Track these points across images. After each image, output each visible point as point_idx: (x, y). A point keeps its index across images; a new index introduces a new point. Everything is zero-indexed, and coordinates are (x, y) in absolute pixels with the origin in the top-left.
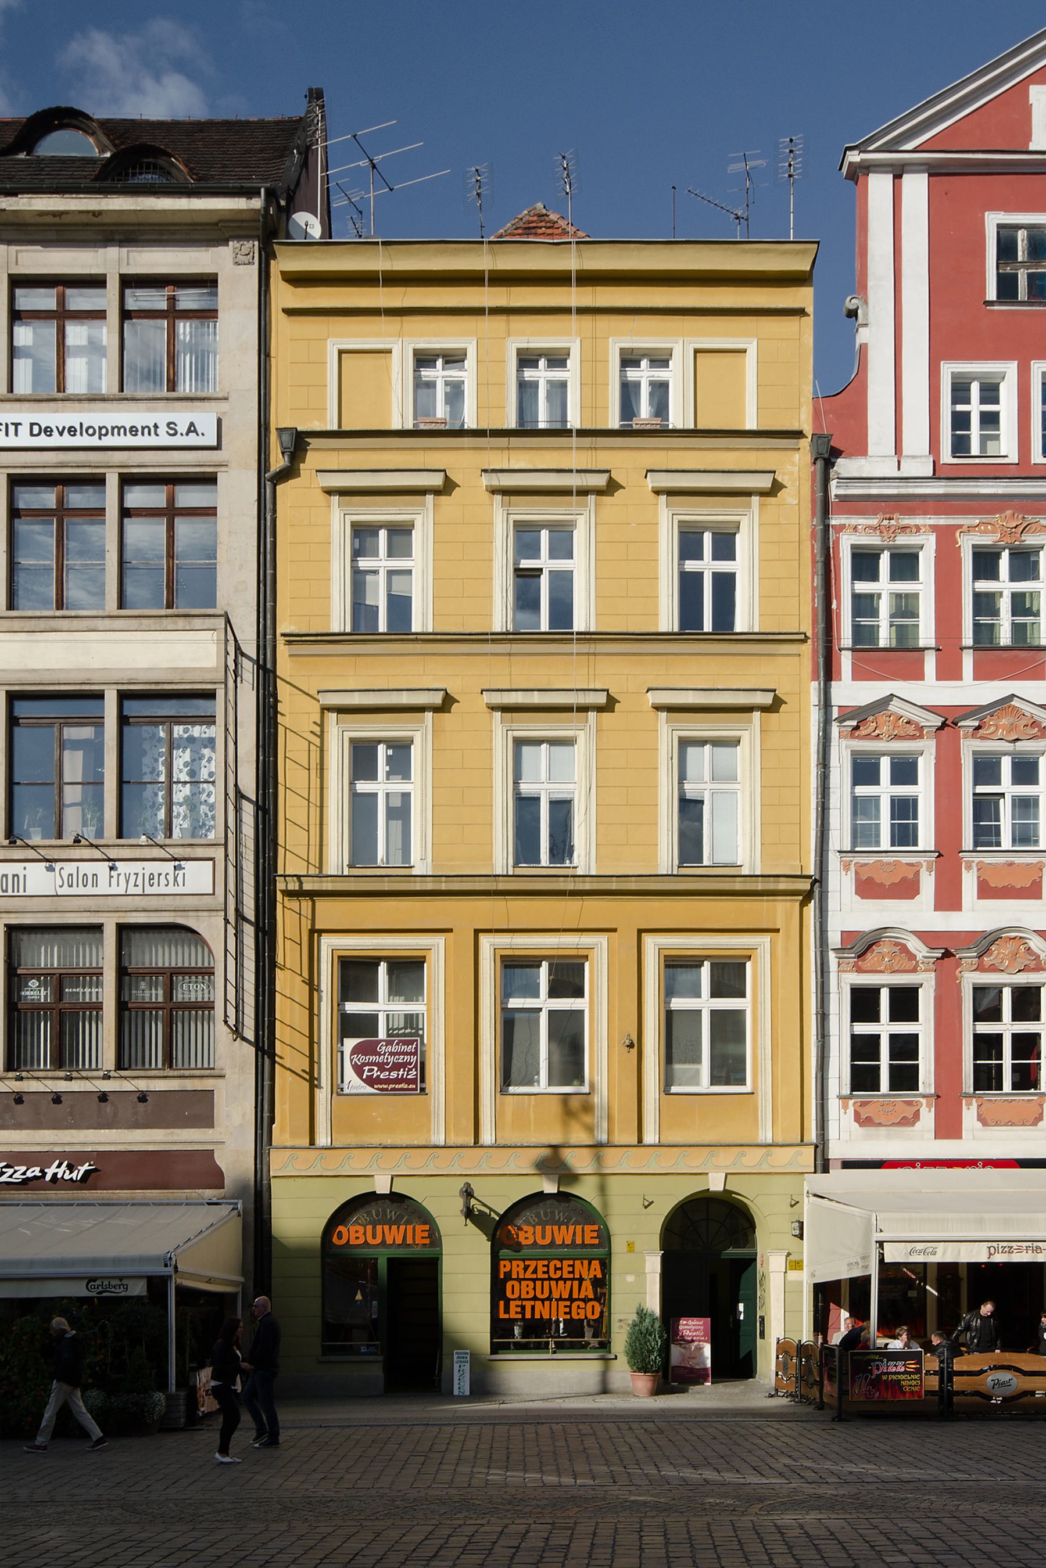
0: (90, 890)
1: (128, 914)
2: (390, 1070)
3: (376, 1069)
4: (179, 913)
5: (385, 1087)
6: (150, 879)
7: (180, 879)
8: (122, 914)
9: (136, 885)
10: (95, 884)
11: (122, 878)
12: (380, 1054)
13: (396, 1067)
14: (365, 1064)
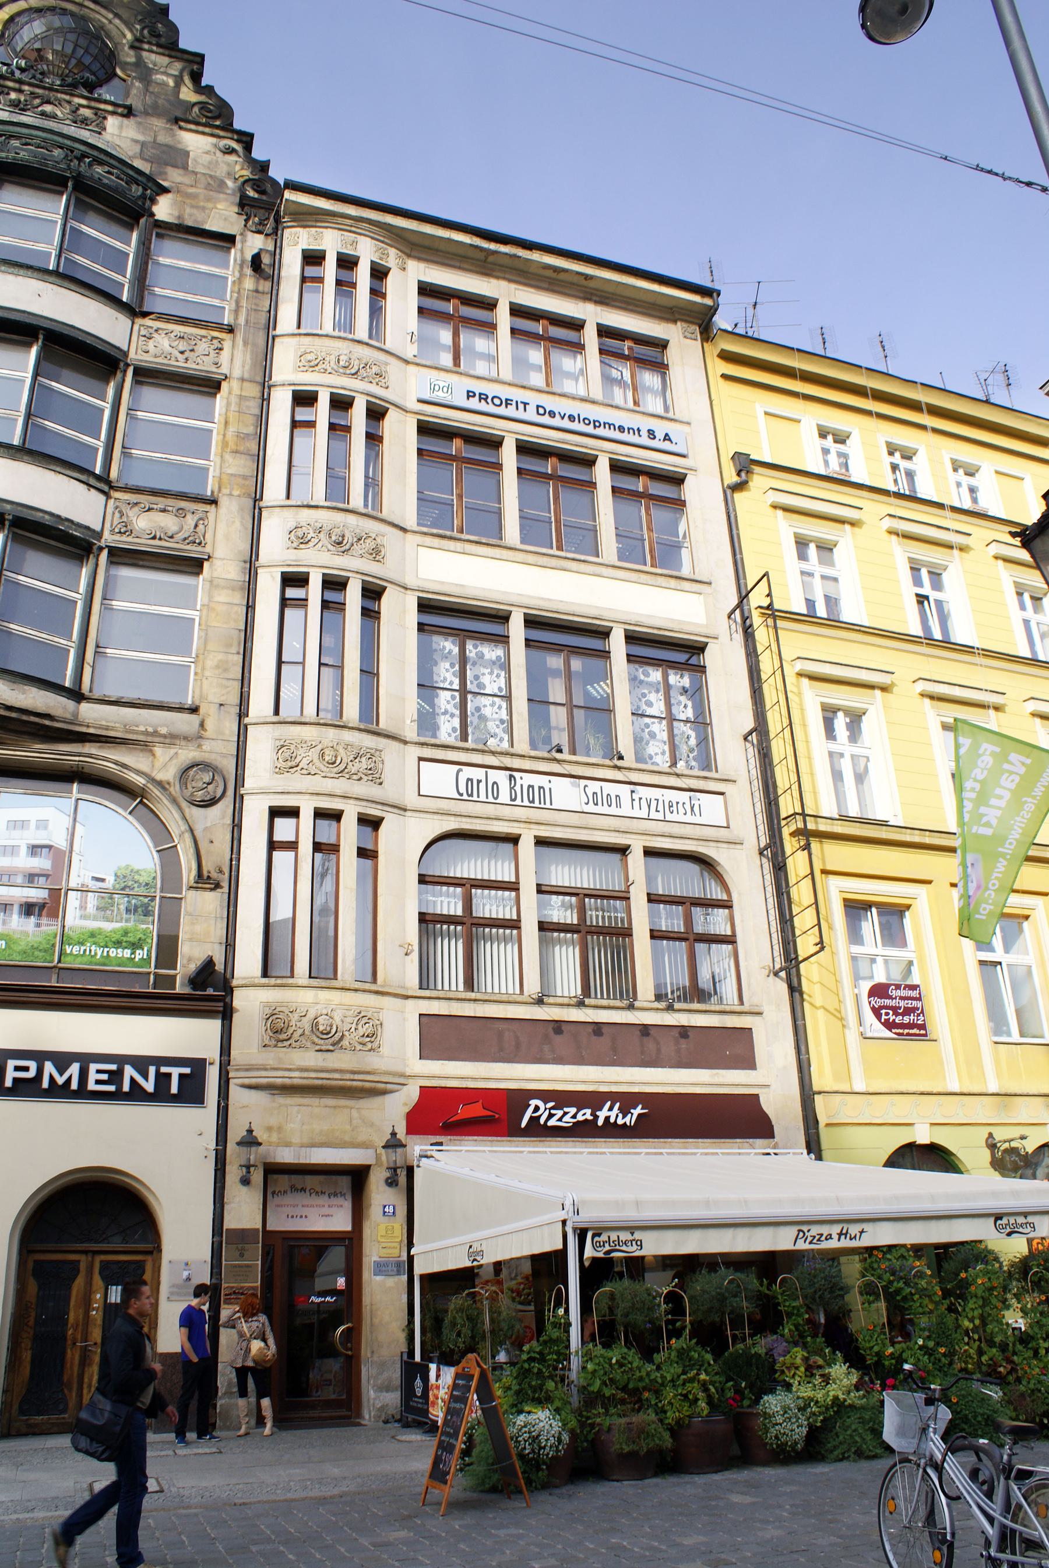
0: (613, 810)
1: (654, 838)
2: (903, 1014)
3: (891, 1012)
4: (701, 843)
5: (901, 1031)
6: (670, 807)
7: (696, 809)
8: (648, 838)
9: (657, 811)
10: (619, 805)
11: (644, 803)
12: (891, 998)
13: (908, 1011)
14: (881, 1008)
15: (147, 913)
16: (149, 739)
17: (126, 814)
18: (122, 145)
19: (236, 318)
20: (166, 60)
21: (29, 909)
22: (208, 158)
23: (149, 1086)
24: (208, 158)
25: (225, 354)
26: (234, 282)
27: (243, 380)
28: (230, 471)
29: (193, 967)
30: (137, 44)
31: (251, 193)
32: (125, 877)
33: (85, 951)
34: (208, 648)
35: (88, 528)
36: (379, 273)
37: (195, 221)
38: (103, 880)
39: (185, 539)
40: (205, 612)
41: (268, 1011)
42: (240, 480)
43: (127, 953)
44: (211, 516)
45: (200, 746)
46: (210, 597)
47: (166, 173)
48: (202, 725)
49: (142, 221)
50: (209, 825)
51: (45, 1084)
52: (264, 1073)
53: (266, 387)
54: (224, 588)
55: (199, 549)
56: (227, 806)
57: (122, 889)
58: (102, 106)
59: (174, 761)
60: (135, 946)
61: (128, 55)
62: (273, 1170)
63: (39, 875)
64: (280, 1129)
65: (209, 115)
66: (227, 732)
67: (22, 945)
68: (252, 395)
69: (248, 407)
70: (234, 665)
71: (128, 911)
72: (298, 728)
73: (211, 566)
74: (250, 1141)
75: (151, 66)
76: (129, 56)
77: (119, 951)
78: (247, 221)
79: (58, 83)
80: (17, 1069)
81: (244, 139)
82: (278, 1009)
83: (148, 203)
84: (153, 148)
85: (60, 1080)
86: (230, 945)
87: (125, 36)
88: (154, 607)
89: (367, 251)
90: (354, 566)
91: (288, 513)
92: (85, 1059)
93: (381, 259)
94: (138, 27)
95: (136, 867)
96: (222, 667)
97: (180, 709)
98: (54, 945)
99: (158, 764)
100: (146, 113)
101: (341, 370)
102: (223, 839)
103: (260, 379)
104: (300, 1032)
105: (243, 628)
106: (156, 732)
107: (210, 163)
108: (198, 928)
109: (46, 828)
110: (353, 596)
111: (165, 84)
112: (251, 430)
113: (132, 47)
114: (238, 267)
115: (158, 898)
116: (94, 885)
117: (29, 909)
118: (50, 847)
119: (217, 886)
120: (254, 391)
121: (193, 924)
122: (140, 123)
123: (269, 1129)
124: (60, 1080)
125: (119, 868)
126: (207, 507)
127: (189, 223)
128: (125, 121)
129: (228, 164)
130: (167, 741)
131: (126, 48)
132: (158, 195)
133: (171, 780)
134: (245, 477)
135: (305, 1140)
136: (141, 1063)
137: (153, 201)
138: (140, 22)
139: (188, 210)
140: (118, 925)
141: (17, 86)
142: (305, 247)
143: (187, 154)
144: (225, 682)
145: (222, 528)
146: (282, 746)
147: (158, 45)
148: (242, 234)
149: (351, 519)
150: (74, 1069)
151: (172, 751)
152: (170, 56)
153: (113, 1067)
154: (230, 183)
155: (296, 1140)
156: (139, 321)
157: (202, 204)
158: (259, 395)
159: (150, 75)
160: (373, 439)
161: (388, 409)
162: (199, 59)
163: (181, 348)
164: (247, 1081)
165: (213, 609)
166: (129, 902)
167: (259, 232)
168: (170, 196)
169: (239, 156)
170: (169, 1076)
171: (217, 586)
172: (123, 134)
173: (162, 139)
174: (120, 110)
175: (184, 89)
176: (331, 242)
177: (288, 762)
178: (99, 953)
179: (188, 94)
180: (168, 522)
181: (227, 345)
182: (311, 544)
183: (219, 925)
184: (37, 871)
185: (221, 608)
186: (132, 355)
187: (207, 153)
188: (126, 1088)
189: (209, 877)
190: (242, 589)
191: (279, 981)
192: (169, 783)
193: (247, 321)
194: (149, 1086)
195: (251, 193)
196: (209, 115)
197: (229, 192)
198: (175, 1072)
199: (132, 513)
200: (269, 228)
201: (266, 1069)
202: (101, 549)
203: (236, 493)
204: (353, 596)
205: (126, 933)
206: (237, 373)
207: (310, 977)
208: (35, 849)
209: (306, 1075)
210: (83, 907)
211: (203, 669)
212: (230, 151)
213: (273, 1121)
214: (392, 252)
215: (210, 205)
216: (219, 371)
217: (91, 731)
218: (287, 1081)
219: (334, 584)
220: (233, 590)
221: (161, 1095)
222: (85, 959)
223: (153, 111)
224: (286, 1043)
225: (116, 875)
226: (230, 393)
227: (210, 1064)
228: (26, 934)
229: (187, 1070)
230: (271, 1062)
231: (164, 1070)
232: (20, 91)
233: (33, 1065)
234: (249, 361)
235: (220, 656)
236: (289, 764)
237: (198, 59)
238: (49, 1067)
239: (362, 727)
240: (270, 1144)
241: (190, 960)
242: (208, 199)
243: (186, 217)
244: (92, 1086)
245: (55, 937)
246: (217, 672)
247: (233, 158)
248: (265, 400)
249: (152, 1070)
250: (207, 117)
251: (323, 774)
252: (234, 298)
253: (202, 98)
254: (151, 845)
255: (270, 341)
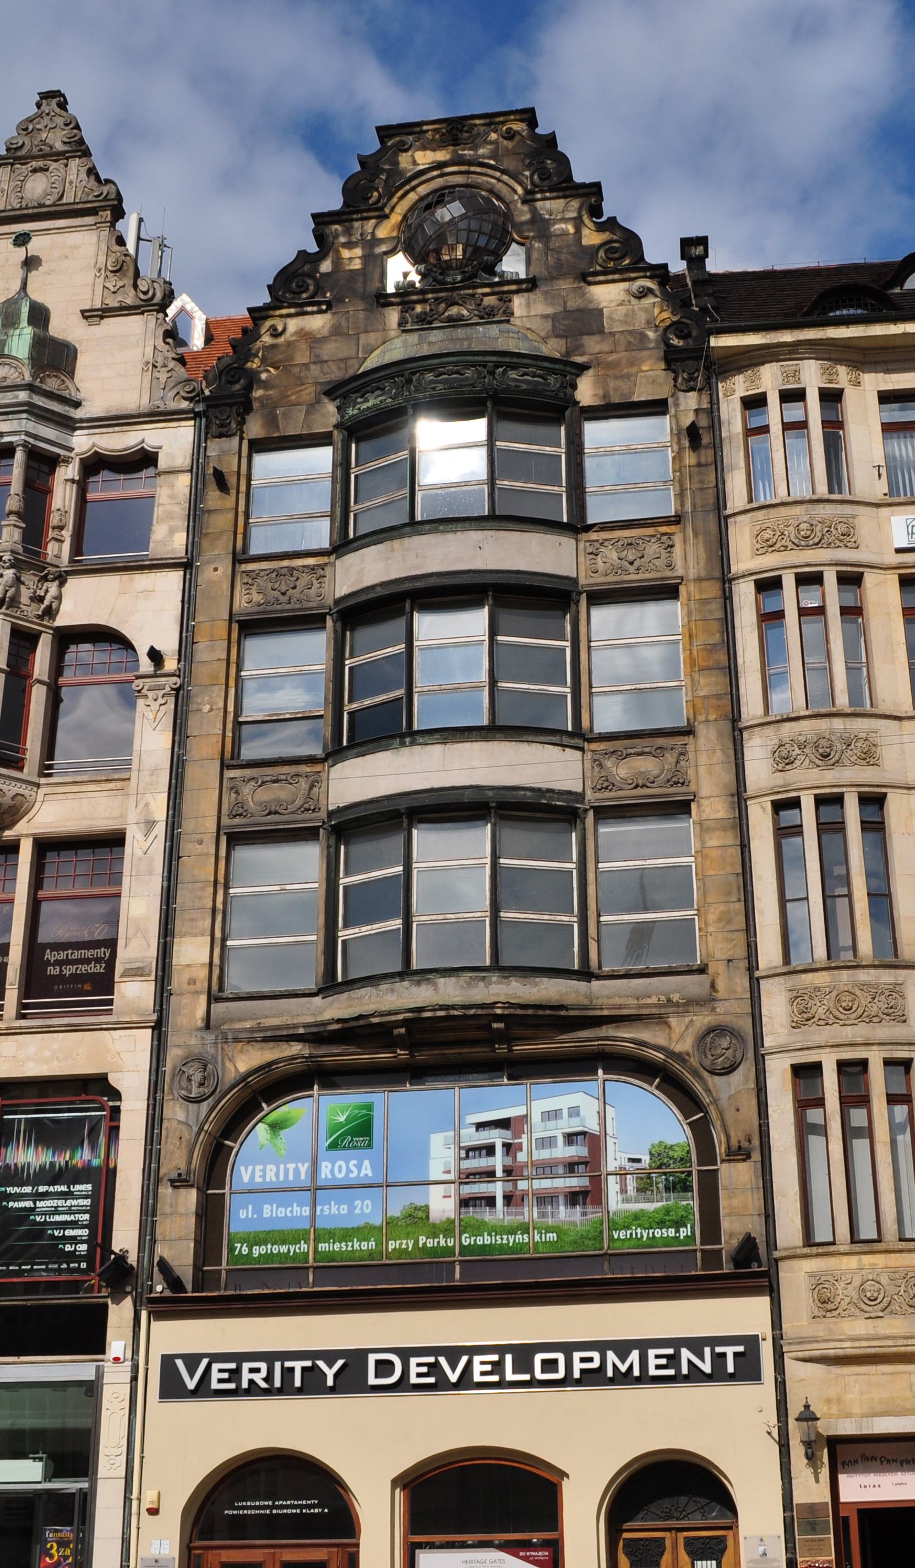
15: (687, 1188)
16: (663, 1011)
17: (652, 1089)
18: (534, 327)
19: (682, 506)
20: (561, 202)
21: (574, 1198)
22: (622, 310)
23: (707, 1368)
24: (622, 310)
25: (678, 550)
26: (674, 458)
27: (699, 580)
28: (702, 694)
29: (735, 1242)
30: (530, 197)
31: (675, 342)
32: (659, 1154)
33: (631, 1234)
34: (708, 901)
35: (569, 793)
36: (831, 397)
37: (623, 395)
38: (639, 1161)
39: (668, 781)
40: (699, 859)
41: (814, 1281)
42: (713, 702)
43: (672, 1232)
44: (690, 748)
45: (713, 1009)
46: (703, 843)
47: (582, 346)
48: (713, 986)
49: (567, 413)
50: (733, 1092)
51: (610, 1373)
52: (816, 1346)
53: (726, 581)
54: (714, 830)
55: (684, 789)
56: (749, 1070)
57: (659, 1167)
58: (506, 288)
59: (691, 1030)
60: (678, 1224)
61: (522, 213)
62: (835, 1443)
63: (578, 1164)
64: (839, 1400)
65: (616, 255)
66: (739, 989)
67: (572, 1236)
68: (712, 596)
69: (711, 612)
70: (736, 914)
71: (667, 1189)
72: (810, 975)
73: (699, 806)
74: (808, 1416)
75: (547, 217)
76: (523, 214)
77: (664, 1230)
78: (675, 380)
79: (459, 278)
80: (583, 1360)
81: (658, 272)
82: (823, 1278)
83: (569, 390)
84: (564, 319)
85: (623, 1368)
86: (769, 1215)
87: (515, 192)
88: (648, 862)
89: (811, 375)
90: (848, 776)
91: (769, 731)
92: (644, 1345)
93: (831, 382)
94: (527, 173)
95: (670, 1142)
96: (725, 918)
97: (690, 972)
98: (601, 1232)
99: (675, 1036)
100: (552, 278)
101: (803, 543)
102: (750, 1104)
103: (717, 574)
104: (847, 1300)
105: (740, 871)
106: (669, 1000)
107: (626, 315)
108: (736, 1202)
109: (578, 1115)
110: (852, 812)
111: (565, 233)
112: (717, 638)
113: (525, 202)
114: (675, 439)
115: (695, 1174)
116: (629, 1166)
117: (574, 1198)
118: (584, 1133)
119: (748, 1156)
120: (713, 590)
121: (730, 1198)
122: (547, 293)
123: (828, 1401)
124: (623, 1368)
125: (653, 1146)
126: (685, 740)
127: (615, 400)
128: (531, 296)
129: (646, 310)
130: (681, 1009)
131: (519, 205)
132: (578, 376)
133: (690, 1051)
134: (718, 696)
135: (865, 1411)
136: (696, 1345)
137: (574, 387)
138: (528, 167)
139: (612, 384)
140: (659, 1205)
141: (421, 297)
142: (742, 395)
143: (601, 311)
144: (729, 935)
145: (703, 759)
146: (797, 997)
147: (550, 191)
148: (673, 395)
149: (838, 723)
150: (635, 1356)
151: (687, 1020)
152: (565, 197)
153: (670, 1351)
154: (651, 334)
155: (856, 1410)
156: (584, 536)
157: (625, 371)
158: (720, 593)
159: (549, 229)
160: (852, 612)
161: (862, 573)
162: (594, 190)
163: (631, 558)
164: (800, 1354)
165: (707, 856)
166: (667, 1180)
167: (691, 389)
168: (591, 372)
169: (657, 296)
170: (724, 1355)
171: (708, 830)
172: (532, 314)
173: (573, 304)
174: (524, 286)
175: (585, 232)
176: (770, 379)
177: (803, 1018)
178: (645, 1236)
179: (591, 237)
180: (647, 765)
181: (678, 539)
182: (798, 762)
183: (756, 1196)
184: (576, 1159)
185: (715, 853)
186: (583, 581)
187: (621, 304)
188: (685, 1371)
189: (740, 1148)
190: (733, 827)
191: (821, 1250)
192: (688, 1054)
193: (694, 506)
194: (707, 1368)
195: (675, 342)
196: (616, 255)
197: (652, 345)
198: (730, 1351)
199: (609, 763)
200: (700, 382)
201: (818, 1342)
202: (586, 811)
203: (712, 717)
204: (852, 812)
205: (667, 1211)
206: (692, 573)
207: (852, 1242)
208: (570, 1138)
209: (857, 1344)
210: (623, 1190)
211: (706, 924)
212: (643, 293)
213: (832, 1393)
214: (842, 370)
215: (634, 370)
216: (675, 574)
217: (606, 1013)
218: (840, 1352)
219: (829, 801)
220: (724, 830)
221: (718, 1375)
222: (633, 1243)
223: (557, 272)
224: (835, 1313)
225: (651, 1154)
226: (689, 600)
227: (764, 1339)
228: (574, 1223)
229: (741, 1349)
230: (821, 1334)
231: (719, 1350)
232: (424, 301)
233: (596, 1355)
234: (703, 555)
235: (722, 908)
236: (805, 1016)
237: (594, 190)
238: (611, 1356)
239: (877, 963)
240: (831, 1416)
241: (731, 1235)
242: (632, 363)
243: (612, 393)
244: (653, 1372)
245: (602, 1224)
246: (720, 925)
247: (650, 300)
248: (727, 598)
249: (707, 1351)
250: (614, 260)
251: (842, 1022)
252: (677, 479)
253: (606, 236)
254: (681, 1118)
255: (723, 521)
